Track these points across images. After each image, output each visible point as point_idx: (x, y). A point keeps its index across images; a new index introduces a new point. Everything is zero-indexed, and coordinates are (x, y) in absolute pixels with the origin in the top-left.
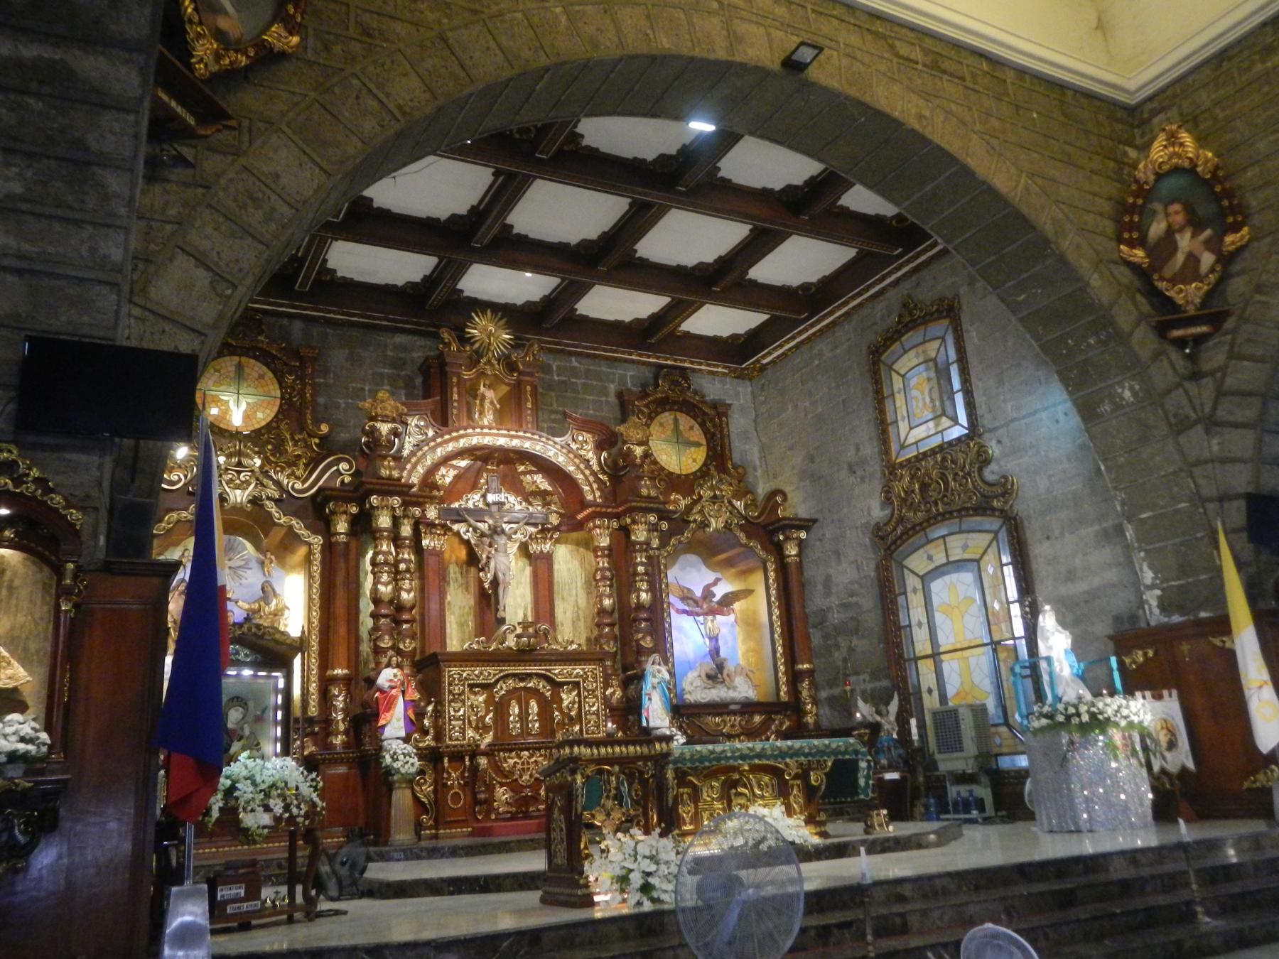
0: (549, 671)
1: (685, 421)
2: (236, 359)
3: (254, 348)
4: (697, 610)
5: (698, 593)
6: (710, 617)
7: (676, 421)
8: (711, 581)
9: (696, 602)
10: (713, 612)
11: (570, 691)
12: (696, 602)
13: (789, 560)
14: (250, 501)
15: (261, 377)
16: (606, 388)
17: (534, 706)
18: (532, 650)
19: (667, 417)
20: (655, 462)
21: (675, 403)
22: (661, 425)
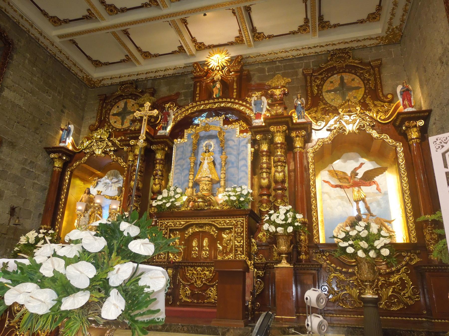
0: (214, 221)
1: (347, 77)
2: (125, 100)
3: (131, 94)
4: (347, 185)
5: (349, 174)
6: (356, 189)
7: (342, 79)
8: (357, 165)
9: (348, 180)
10: (357, 184)
11: (228, 234)
12: (348, 180)
13: (411, 143)
14: (103, 153)
15: (133, 105)
16: (297, 71)
17: (205, 242)
18: (201, 210)
19: (336, 78)
20: (326, 103)
21: (343, 68)
22: (331, 82)
